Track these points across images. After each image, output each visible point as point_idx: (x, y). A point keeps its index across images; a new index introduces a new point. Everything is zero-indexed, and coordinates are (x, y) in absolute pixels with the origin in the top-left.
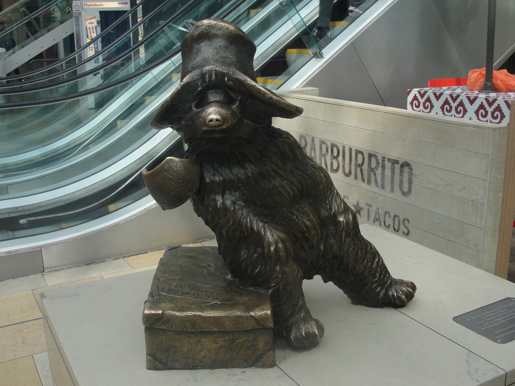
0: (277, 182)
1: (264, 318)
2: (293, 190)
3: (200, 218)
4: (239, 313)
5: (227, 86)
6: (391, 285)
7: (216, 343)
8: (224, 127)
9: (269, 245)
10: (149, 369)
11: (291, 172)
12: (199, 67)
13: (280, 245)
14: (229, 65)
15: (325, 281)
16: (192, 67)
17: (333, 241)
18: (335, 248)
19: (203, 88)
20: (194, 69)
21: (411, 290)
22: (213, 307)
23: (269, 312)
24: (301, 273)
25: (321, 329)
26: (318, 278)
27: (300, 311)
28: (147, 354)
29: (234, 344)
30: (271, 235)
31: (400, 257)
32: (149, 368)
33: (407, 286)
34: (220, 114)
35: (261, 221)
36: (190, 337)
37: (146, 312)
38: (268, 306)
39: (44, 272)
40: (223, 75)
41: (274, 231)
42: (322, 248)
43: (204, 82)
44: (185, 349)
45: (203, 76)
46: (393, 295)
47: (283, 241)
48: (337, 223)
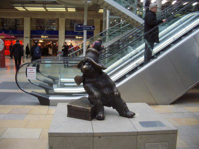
0: (99, 83)
1: (89, 109)
2: (103, 85)
4: (84, 107)
5: (89, 62)
6: (128, 112)
24: (101, 103)
26: (112, 108)
30: (96, 93)
31: (131, 107)
32: (68, 116)
40: (88, 59)
45: (85, 59)
47: (98, 95)
48: (114, 94)
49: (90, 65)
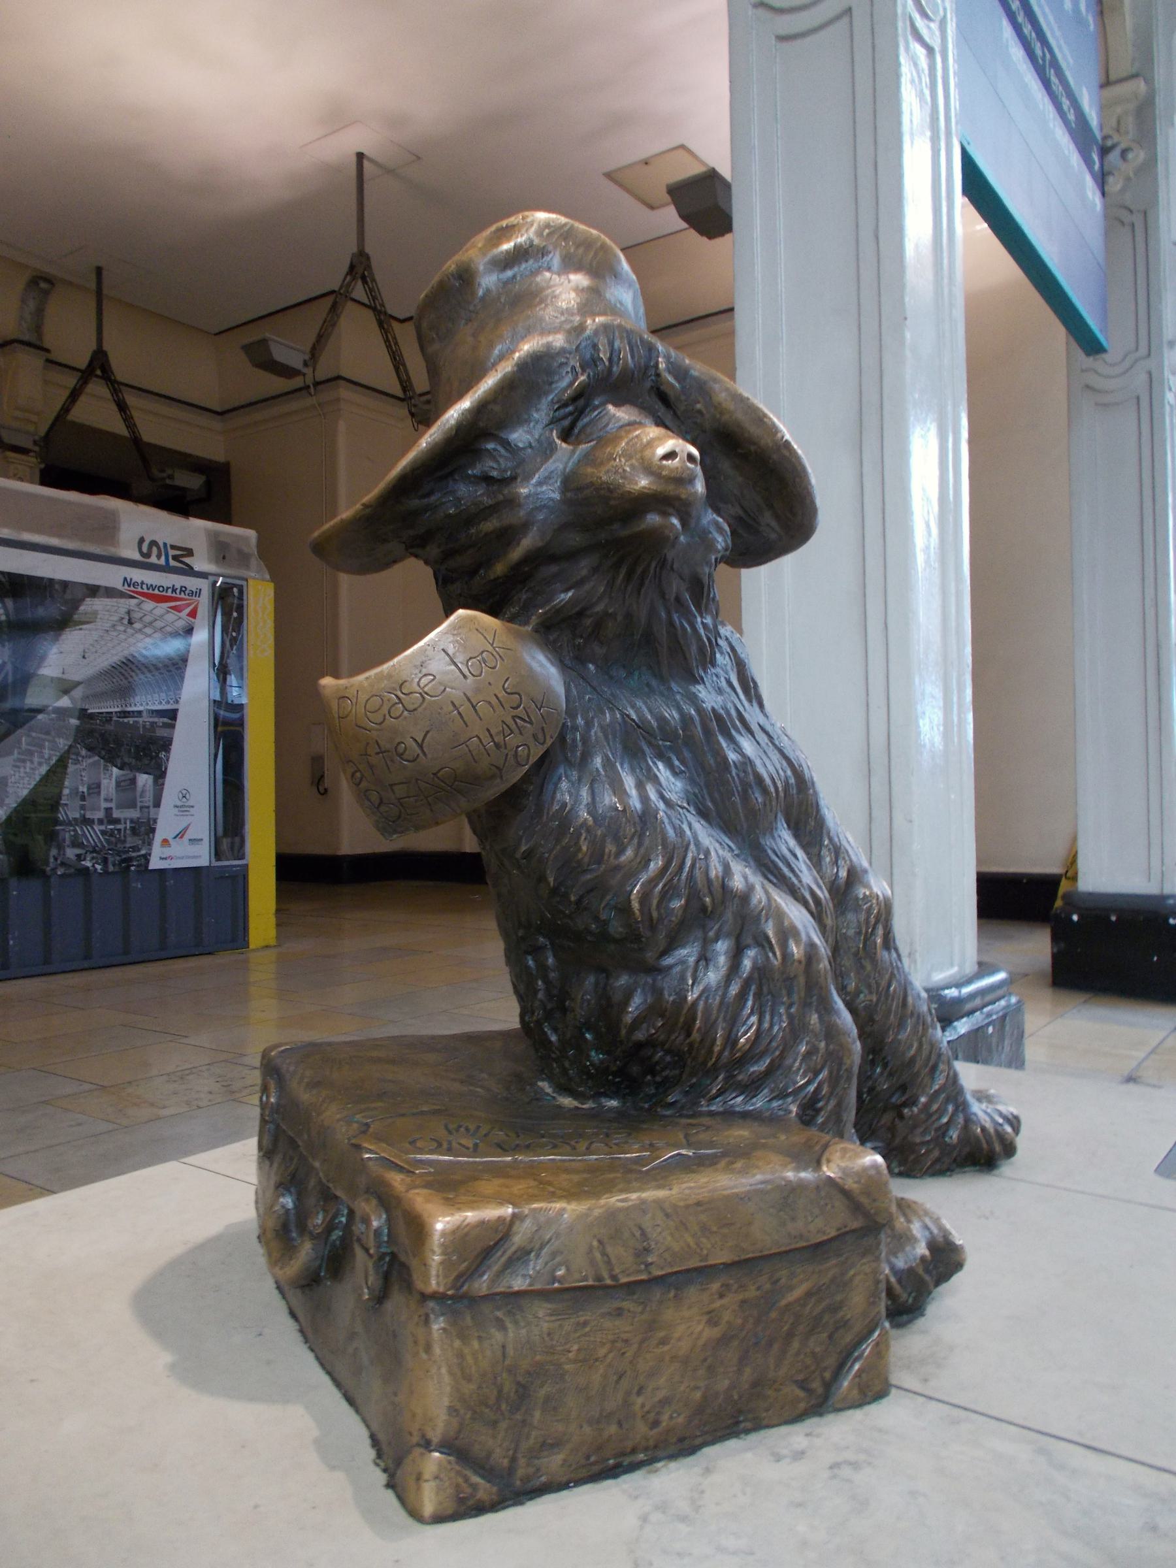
7: (712, 1319)
29: (773, 1315)
36: (619, 1312)
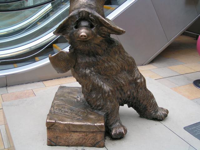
1: (101, 126)
3: (75, 78)
4: (89, 124)
5: (90, 19)
7: (78, 136)
8: (88, 39)
9: (105, 93)
10: (48, 145)
11: (118, 60)
12: (78, 9)
13: (110, 93)
14: (92, 8)
15: (129, 107)
16: (74, 8)
17: (134, 91)
18: (135, 94)
19: (79, 19)
20: (75, 9)
21: (166, 113)
22: (78, 120)
23: (103, 124)
25: (126, 131)
26: (126, 106)
27: (116, 122)
28: (48, 139)
30: (106, 88)
33: (165, 111)
34: (86, 33)
35: (102, 81)
37: (47, 121)
38: (103, 121)
39: (7, 86)
40: (89, 13)
41: (108, 87)
42: (129, 93)
43: (79, 16)
44: (65, 138)
45: (79, 13)
46: (158, 115)
47: (112, 91)
49: (91, 26)
